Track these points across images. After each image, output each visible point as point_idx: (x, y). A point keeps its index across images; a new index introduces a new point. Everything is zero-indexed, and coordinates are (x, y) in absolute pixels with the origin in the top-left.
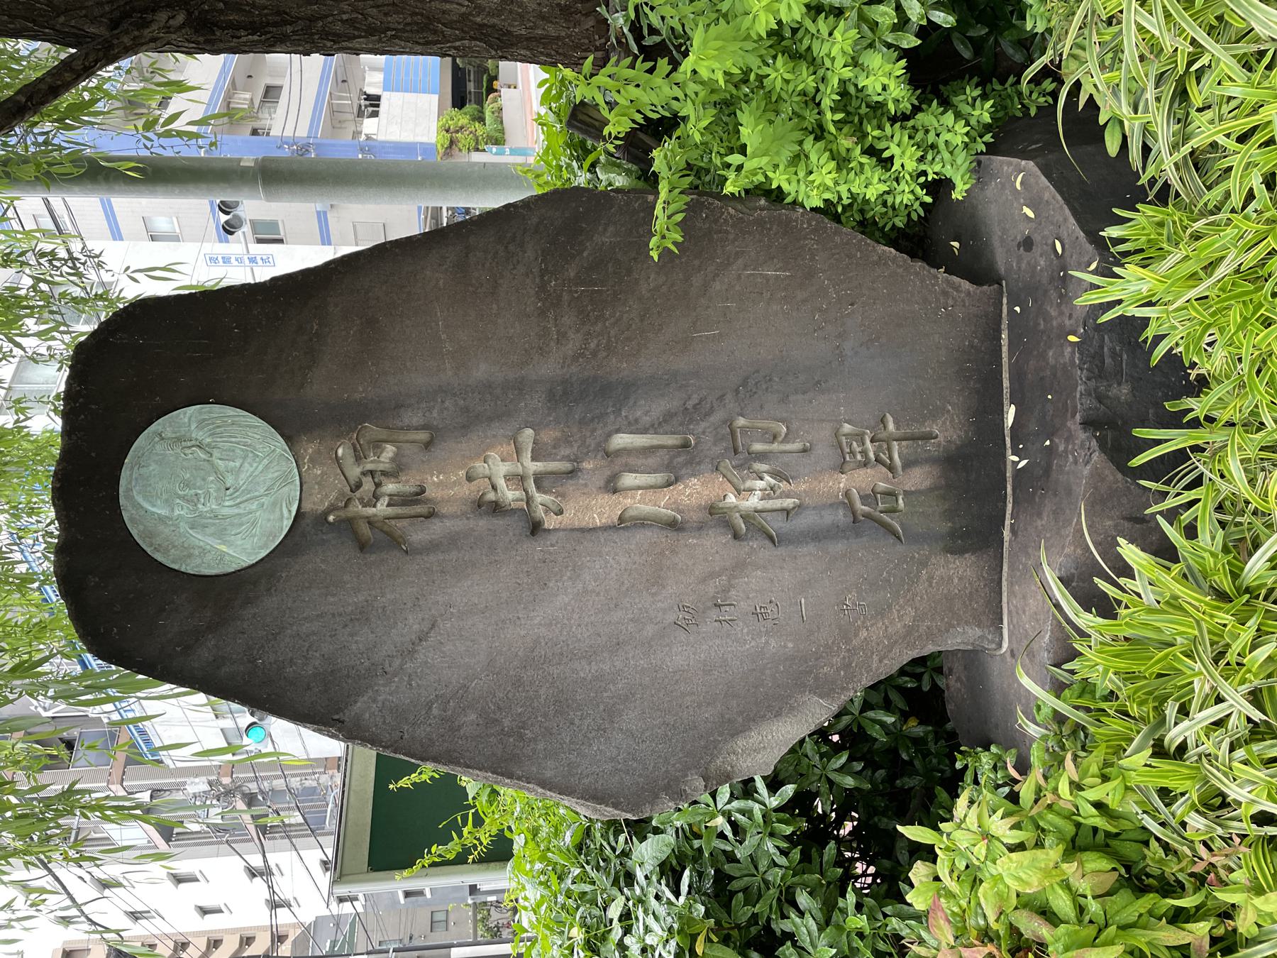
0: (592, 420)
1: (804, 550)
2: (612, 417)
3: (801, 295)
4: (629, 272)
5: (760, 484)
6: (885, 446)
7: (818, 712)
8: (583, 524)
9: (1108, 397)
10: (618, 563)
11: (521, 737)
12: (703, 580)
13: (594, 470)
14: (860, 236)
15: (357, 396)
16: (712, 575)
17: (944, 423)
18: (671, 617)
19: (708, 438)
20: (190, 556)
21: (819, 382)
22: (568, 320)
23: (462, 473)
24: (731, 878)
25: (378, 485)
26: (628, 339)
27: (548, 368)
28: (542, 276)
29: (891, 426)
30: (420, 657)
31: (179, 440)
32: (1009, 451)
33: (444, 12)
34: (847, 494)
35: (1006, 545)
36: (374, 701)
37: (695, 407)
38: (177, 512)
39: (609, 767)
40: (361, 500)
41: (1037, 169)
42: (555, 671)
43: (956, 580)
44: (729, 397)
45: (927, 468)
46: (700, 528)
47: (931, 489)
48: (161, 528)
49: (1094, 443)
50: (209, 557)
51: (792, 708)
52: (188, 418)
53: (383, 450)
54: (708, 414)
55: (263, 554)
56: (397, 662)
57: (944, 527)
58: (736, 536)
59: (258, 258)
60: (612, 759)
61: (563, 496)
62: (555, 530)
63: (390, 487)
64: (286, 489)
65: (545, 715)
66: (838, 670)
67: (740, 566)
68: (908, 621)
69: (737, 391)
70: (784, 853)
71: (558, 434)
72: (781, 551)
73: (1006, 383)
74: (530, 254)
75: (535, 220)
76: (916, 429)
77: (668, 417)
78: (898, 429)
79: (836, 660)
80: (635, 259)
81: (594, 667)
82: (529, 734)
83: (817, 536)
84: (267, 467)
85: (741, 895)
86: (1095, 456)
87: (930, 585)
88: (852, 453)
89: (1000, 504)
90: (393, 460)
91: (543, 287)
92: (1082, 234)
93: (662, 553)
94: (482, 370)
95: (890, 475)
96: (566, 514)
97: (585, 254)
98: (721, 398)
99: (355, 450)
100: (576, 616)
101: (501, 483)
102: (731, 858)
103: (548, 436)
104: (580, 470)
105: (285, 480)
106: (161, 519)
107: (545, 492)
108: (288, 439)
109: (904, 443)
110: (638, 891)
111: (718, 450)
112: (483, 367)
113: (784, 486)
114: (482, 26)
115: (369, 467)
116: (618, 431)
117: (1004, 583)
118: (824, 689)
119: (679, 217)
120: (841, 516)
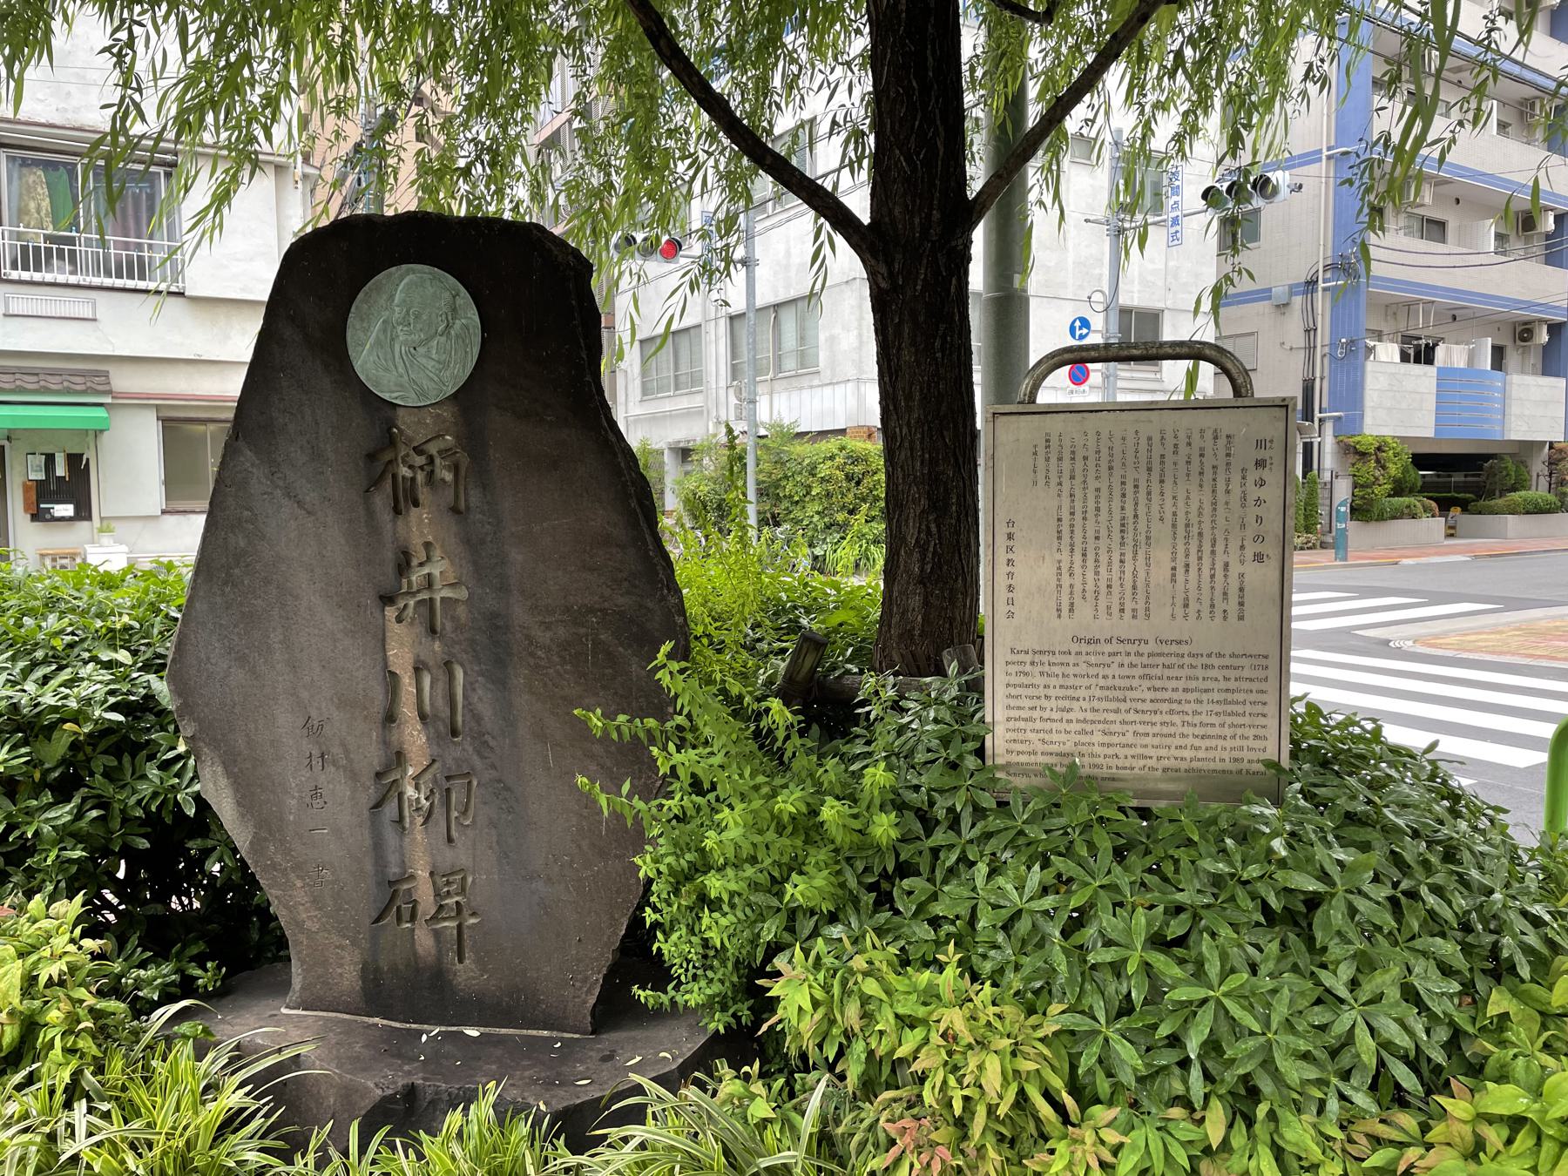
0: (474, 651)
1: (367, 833)
2: (476, 668)
3: (585, 844)
4: (604, 687)
5: (422, 797)
6: (453, 914)
7: (241, 835)
8: (388, 641)
9: (435, 1110)
10: (358, 670)
11: (225, 583)
12: (343, 745)
13: (433, 651)
14: (636, 902)
15: (491, 452)
16: (347, 751)
17: (472, 971)
18: (314, 714)
19: (458, 753)
20: (362, 320)
21: (508, 857)
22: (561, 632)
23: (430, 539)
24: (133, 757)
25: (421, 468)
26: (545, 685)
27: (519, 613)
28: (600, 610)
29: (473, 921)
30: (285, 502)
31: (454, 310)
32: (443, 1029)
33: (907, 521)
34: (412, 877)
35: (366, 1019)
36: (253, 465)
37: (486, 742)
38: (397, 309)
39: (203, 656)
40: (407, 455)
41: (667, 1070)
42: (275, 612)
43: (339, 971)
44: (494, 773)
45: (433, 952)
46: (385, 743)
47: (415, 953)
48: (385, 297)
49: (391, 1092)
50: (361, 334)
51: (243, 816)
52: (471, 316)
53: (449, 471)
54: (479, 753)
55: (363, 378)
56: (281, 483)
57: (385, 966)
58: (379, 775)
59: (1178, 228)
60: (208, 659)
61: (411, 624)
62: (384, 616)
63: (420, 477)
64: (414, 395)
65: (241, 604)
66: (271, 859)
67: (353, 776)
68: (308, 924)
69: (499, 781)
70: (139, 802)
71: (463, 620)
72: (366, 813)
73: (503, 1031)
74: (621, 600)
75: (650, 605)
76: (467, 943)
77: (478, 718)
78: (468, 927)
79: (278, 858)
80: (616, 693)
81: (277, 646)
82: (228, 589)
83: (378, 846)
84: (432, 379)
85: (116, 763)
86: (379, 1092)
87: (337, 947)
88: (448, 883)
89: (401, 1017)
90: (443, 480)
91: (591, 611)
92: (579, 1101)
93: (365, 708)
94: (517, 556)
95: (428, 917)
96: (396, 626)
97: (621, 649)
98: (493, 767)
99: (447, 450)
100: (316, 631)
101: (426, 570)
102: (151, 757)
103: (462, 612)
104: (433, 639)
105: (422, 394)
106: (392, 297)
107: (415, 608)
108: (455, 396)
109: (455, 932)
110: (135, 675)
111: (450, 762)
112: (520, 558)
113: (420, 820)
114: (898, 555)
115: (438, 461)
116: (465, 673)
117: (334, 1014)
118: (257, 844)
119: (615, 736)
120: (394, 870)
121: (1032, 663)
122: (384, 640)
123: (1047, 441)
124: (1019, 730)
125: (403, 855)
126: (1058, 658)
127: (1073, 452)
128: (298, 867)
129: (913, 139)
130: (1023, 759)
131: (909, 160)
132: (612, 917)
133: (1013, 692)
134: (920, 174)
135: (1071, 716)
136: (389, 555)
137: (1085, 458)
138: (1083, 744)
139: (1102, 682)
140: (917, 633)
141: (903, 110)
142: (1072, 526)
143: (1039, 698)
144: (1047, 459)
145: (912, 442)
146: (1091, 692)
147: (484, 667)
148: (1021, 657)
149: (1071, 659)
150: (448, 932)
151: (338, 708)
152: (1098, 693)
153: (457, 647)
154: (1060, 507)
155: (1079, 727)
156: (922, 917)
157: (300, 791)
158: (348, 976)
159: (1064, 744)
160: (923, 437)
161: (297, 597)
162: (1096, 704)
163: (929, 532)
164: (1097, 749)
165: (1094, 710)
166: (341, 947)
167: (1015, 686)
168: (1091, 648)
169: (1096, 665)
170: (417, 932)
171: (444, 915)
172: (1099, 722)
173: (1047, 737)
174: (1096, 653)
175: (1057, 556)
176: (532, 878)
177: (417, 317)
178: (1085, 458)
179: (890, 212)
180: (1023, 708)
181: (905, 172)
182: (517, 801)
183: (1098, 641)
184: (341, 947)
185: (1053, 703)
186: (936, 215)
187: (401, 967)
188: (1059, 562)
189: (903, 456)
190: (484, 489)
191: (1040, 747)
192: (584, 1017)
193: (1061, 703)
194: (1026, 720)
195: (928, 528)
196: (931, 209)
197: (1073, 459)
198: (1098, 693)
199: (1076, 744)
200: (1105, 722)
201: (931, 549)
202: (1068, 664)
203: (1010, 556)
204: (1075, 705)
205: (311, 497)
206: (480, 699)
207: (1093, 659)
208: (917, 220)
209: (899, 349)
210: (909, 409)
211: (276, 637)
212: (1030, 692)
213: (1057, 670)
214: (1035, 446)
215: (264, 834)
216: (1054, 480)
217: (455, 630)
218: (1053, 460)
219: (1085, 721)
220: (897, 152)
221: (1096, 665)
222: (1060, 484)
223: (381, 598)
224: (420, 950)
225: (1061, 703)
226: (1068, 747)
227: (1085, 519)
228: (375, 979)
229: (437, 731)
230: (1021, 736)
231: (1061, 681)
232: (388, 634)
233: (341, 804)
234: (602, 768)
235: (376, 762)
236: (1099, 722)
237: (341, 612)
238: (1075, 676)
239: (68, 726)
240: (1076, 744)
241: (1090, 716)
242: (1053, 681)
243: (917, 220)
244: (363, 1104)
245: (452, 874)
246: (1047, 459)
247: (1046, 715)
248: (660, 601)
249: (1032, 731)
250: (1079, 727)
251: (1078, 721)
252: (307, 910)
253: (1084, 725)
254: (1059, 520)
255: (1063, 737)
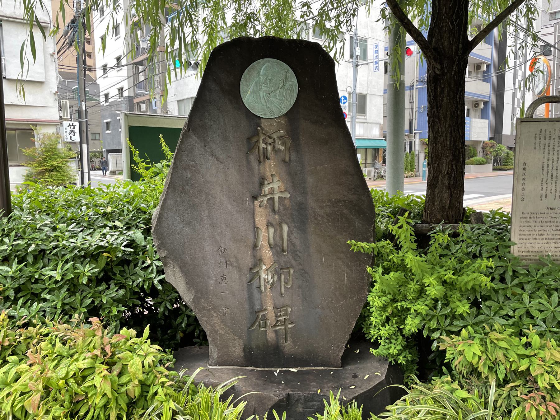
0: (292, 218)
1: (246, 293)
2: (294, 225)
3: (337, 293)
4: (345, 231)
5: (270, 278)
6: (283, 324)
7: (188, 298)
8: (256, 214)
9: (298, 403)
10: (242, 227)
11: (182, 192)
12: (236, 257)
13: (275, 218)
14: (359, 315)
15: (301, 137)
16: (237, 260)
17: (291, 345)
18: (222, 245)
19: (286, 259)
20: (247, 82)
21: (306, 300)
22: (328, 210)
23: (274, 173)
24: (128, 266)
25: (270, 144)
26: (321, 231)
27: (311, 203)
28: (343, 201)
29: (290, 326)
30: (210, 158)
31: (286, 78)
32: (280, 369)
33: (442, 164)
34: (266, 309)
35: (247, 368)
36: (196, 143)
37: (297, 254)
38: (261, 77)
39: (170, 223)
40: (265, 139)
41: (382, 380)
42: (205, 204)
43: (234, 349)
44: (301, 267)
45: (275, 339)
46: (254, 256)
47: (267, 340)
48: (256, 72)
49: (281, 398)
50: (246, 88)
51: (189, 289)
52: (294, 81)
53: (282, 146)
54: (294, 259)
55: (247, 106)
56: (209, 150)
57: (254, 345)
58: (251, 269)
59: (377, 65)
60: (173, 224)
61: (266, 208)
62: (254, 205)
63: (269, 148)
64: (269, 113)
65: (189, 201)
66: (203, 305)
67: (240, 270)
68: (220, 331)
69: (303, 270)
70: (138, 285)
71: (288, 206)
72: (246, 285)
73: (305, 368)
74: (351, 197)
75: (363, 198)
76: (289, 335)
77: (293, 245)
78: (289, 328)
79: (206, 305)
80: (350, 234)
81: (205, 218)
82: (183, 195)
83: (251, 299)
84: (276, 107)
85: (123, 269)
86: (277, 398)
87: (232, 340)
88: (281, 311)
89: (261, 366)
90: (279, 149)
91: (340, 201)
92: (356, 395)
93: (245, 242)
94: (310, 180)
95: (272, 325)
96: (259, 208)
97: (351, 216)
98: (300, 264)
99: (282, 137)
100: (224, 212)
101: (271, 186)
102: (136, 266)
103: (287, 202)
104: (275, 214)
105: (272, 113)
106: (259, 72)
107: (267, 201)
108: (286, 114)
109: (284, 331)
110: (124, 232)
111: (282, 263)
112: (311, 180)
113: (269, 286)
114: (438, 178)
115: (277, 141)
116: (289, 227)
117: (233, 367)
118: (196, 300)
119: (362, 251)
120: (258, 307)
121: (530, 218)
122: (254, 214)
123: (540, 132)
124: (523, 243)
125: (261, 301)
126: (540, 216)
127: (550, 137)
128: (215, 309)
129: (454, 16)
130: (524, 254)
131: (452, 24)
132: (349, 322)
133: (522, 229)
134: (456, 29)
135: (544, 237)
136: (256, 180)
137: (554, 139)
138: (548, 248)
139: (555, 224)
140: (447, 207)
141: (451, 4)
142: (548, 165)
143: (532, 231)
144: (540, 139)
145: (446, 134)
146: (551, 228)
147: (296, 224)
148: (526, 215)
149: (545, 216)
150: (281, 331)
151: (233, 243)
152: (554, 228)
153: (285, 217)
154: (544, 158)
155: (546, 241)
156: (497, 315)
157: (216, 277)
158: (237, 350)
159: (540, 248)
160: (451, 132)
161: (215, 198)
162: (553, 232)
163: (452, 169)
164: (552, 249)
165: (552, 235)
166: (235, 340)
167: (523, 226)
168: (552, 211)
169: (554, 218)
170: (268, 331)
171: (279, 323)
172: (554, 239)
173: (534, 245)
174: (554, 213)
175: (542, 177)
176: (316, 308)
177: (271, 81)
178: (554, 139)
179: (443, 44)
180: (526, 235)
181: (450, 28)
182: (310, 277)
183: (555, 208)
184: (235, 340)
185: (537, 233)
186: (461, 46)
187: (261, 346)
188: (543, 179)
189: (442, 139)
190: (298, 153)
191: (531, 249)
192: (338, 361)
193: (540, 233)
194: (526, 239)
195: (452, 167)
196: (459, 43)
197: (550, 139)
198: (554, 228)
199: (544, 248)
200: (556, 239)
201: (453, 175)
202: (544, 218)
203: (524, 177)
204: (545, 233)
205: (222, 156)
206: (295, 237)
207: (553, 215)
208: (454, 47)
209: (443, 98)
210: (445, 121)
211: (205, 214)
212: (529, 228)
213: (539, 220)
214: (536, 134)
215: (200, 295)
216: (542, 147)
217: (284, 210)
218: (542, 140)
219: (549, 239)
220: (448, 20)
221: (554, 218)
222: (544, 149)
223: (253, 197)
224: (269, 339)
225: (540, 233)
226: (542, 249)
227: (553, 162)
228: (249, 351)
229: (276, 251)
230: (524, 245)
231: (541, 224)
232: (256, 212)
233: (235, 282)
234: (344, 263)
235: (250, 264)
236: (554, 239)
237: (235, 203)
238: (546, 222)
239: (104, 254)
240: (544, 248)
241: (550, 237)
242: (537, 224)
243: (454, 47)
244: (269, 404)
245: (283, 307)
246: (540, 139)
247: (534, 237)
248: (367, 197)
249: (529, 243)
250: (546, 241)
251: (546, 239)
252: (219, 325)
253: (548, 241)
254: (543, 163)
255: (540, 245)
